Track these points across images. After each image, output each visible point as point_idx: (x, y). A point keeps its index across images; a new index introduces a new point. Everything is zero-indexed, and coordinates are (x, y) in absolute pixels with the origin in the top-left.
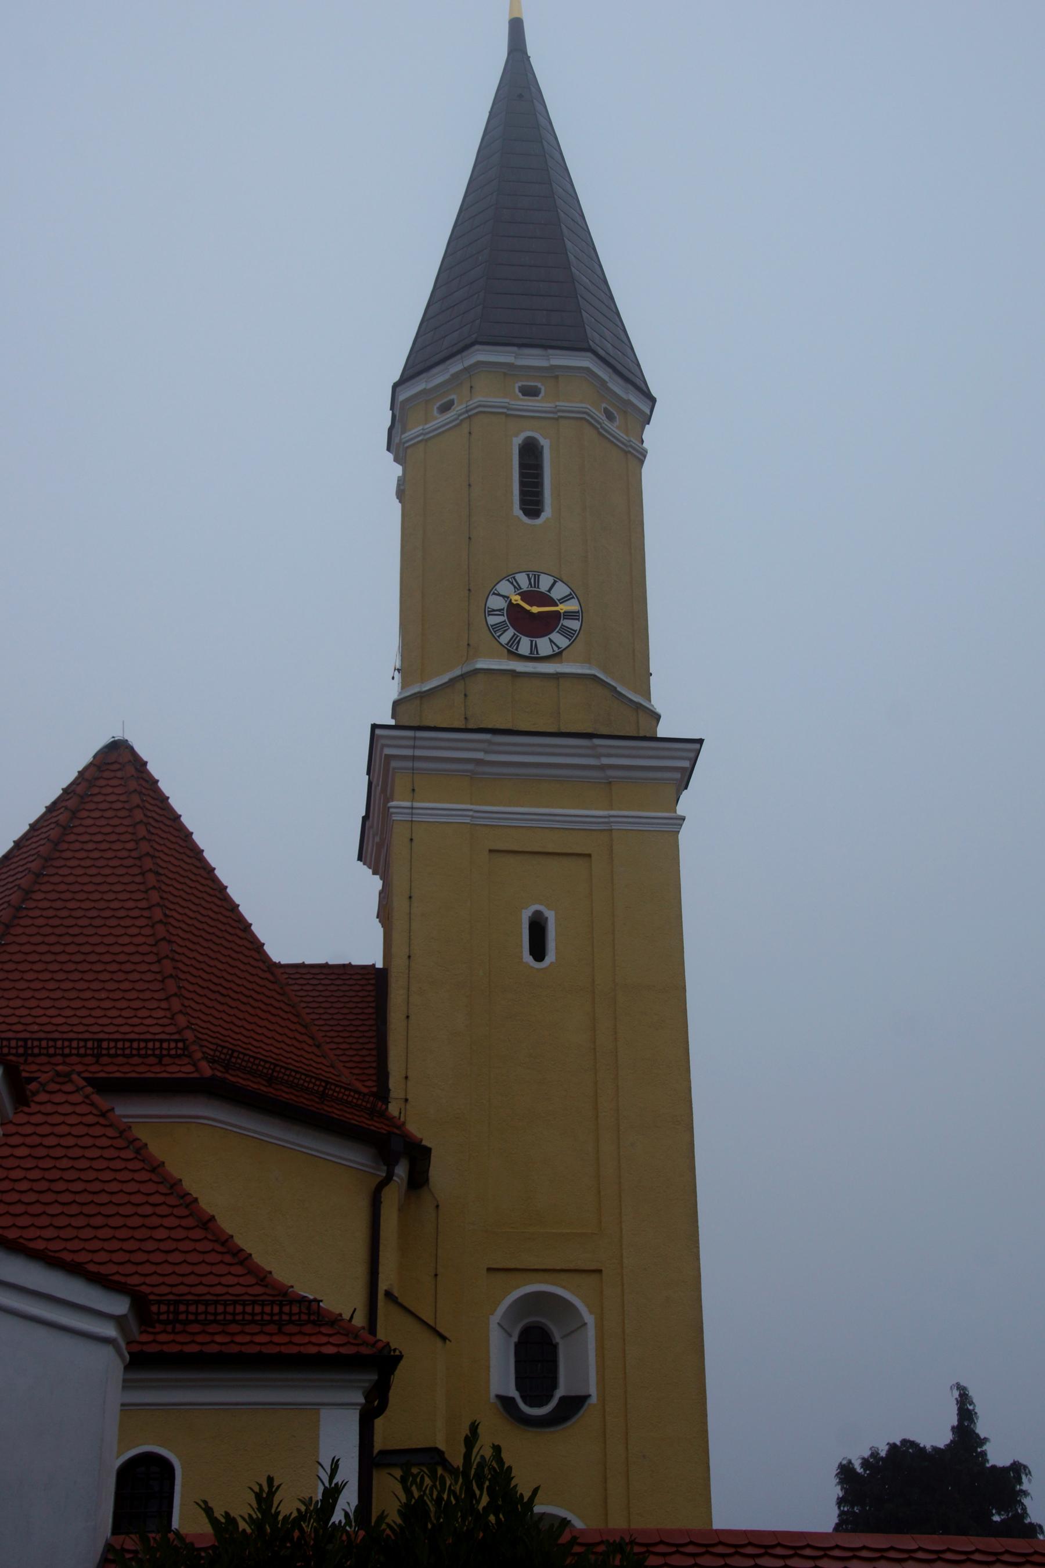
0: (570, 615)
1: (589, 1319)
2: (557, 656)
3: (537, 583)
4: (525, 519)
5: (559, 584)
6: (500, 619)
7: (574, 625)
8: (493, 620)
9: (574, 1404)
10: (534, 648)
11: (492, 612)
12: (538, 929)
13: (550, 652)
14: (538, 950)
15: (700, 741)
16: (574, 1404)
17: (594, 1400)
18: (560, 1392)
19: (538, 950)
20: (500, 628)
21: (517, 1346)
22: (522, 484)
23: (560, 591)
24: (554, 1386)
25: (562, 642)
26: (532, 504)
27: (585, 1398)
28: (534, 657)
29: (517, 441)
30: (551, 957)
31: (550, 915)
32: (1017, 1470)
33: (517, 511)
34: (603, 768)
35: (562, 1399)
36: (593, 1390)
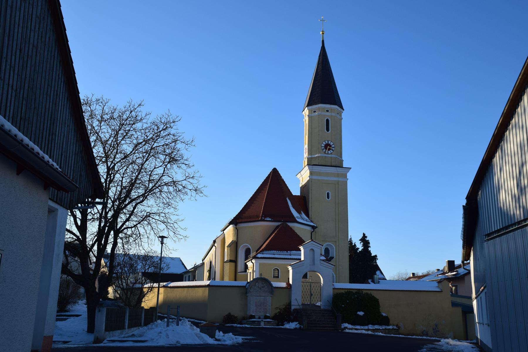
0: (333, 147)
1: (334, 247)
2: (331, 154)
3: (328, 142)
4: (327, 132)
5: (332, 143)
6: (323, 148)
7: (333, 149)
8: (322, 148)
9: (332, 258)
10: (328, 152)
11: (322, 147)
12: (328, 194)
13: (330, 153)
14: (328, 198)
15: (351, 168)
16: (332, 258)
17: (335, 257)
18: (330, 256)
19: (328, 198)
20: (323, 149)
21: (325, 250)
22: (326, 127)
23: (332, 144)
24: (329, 255)
25: (332, 152)
26: (328, 130)
27: (334, 257)
28: (328, 154)
29: (326, 119)
30: (330, 199)
31: (330, 192)
32: (376, 256)
33: (326, 131)
34: (337, 171)
35: (330, 257)
36: (335, 256)
